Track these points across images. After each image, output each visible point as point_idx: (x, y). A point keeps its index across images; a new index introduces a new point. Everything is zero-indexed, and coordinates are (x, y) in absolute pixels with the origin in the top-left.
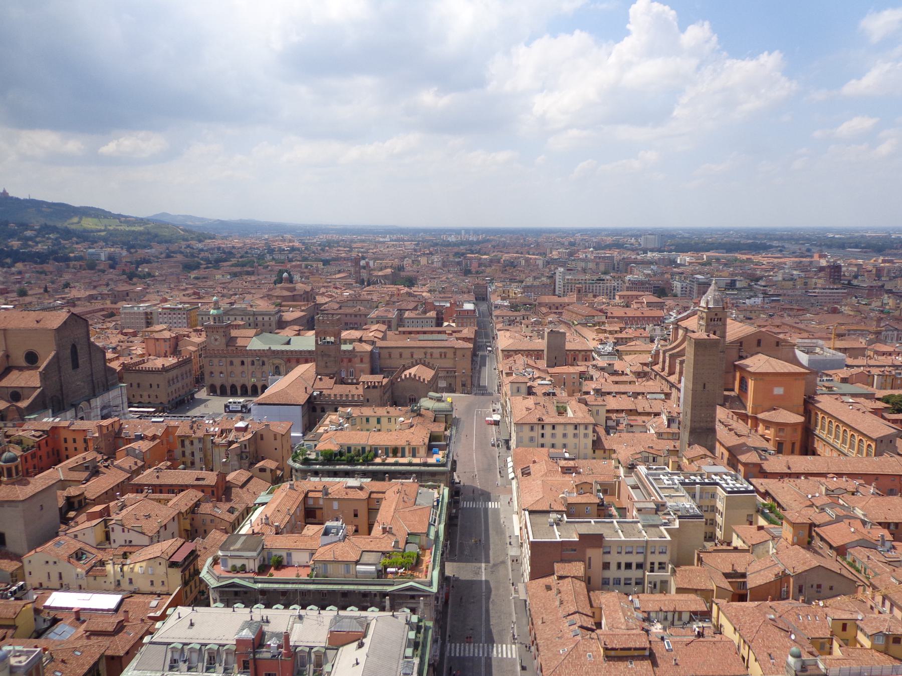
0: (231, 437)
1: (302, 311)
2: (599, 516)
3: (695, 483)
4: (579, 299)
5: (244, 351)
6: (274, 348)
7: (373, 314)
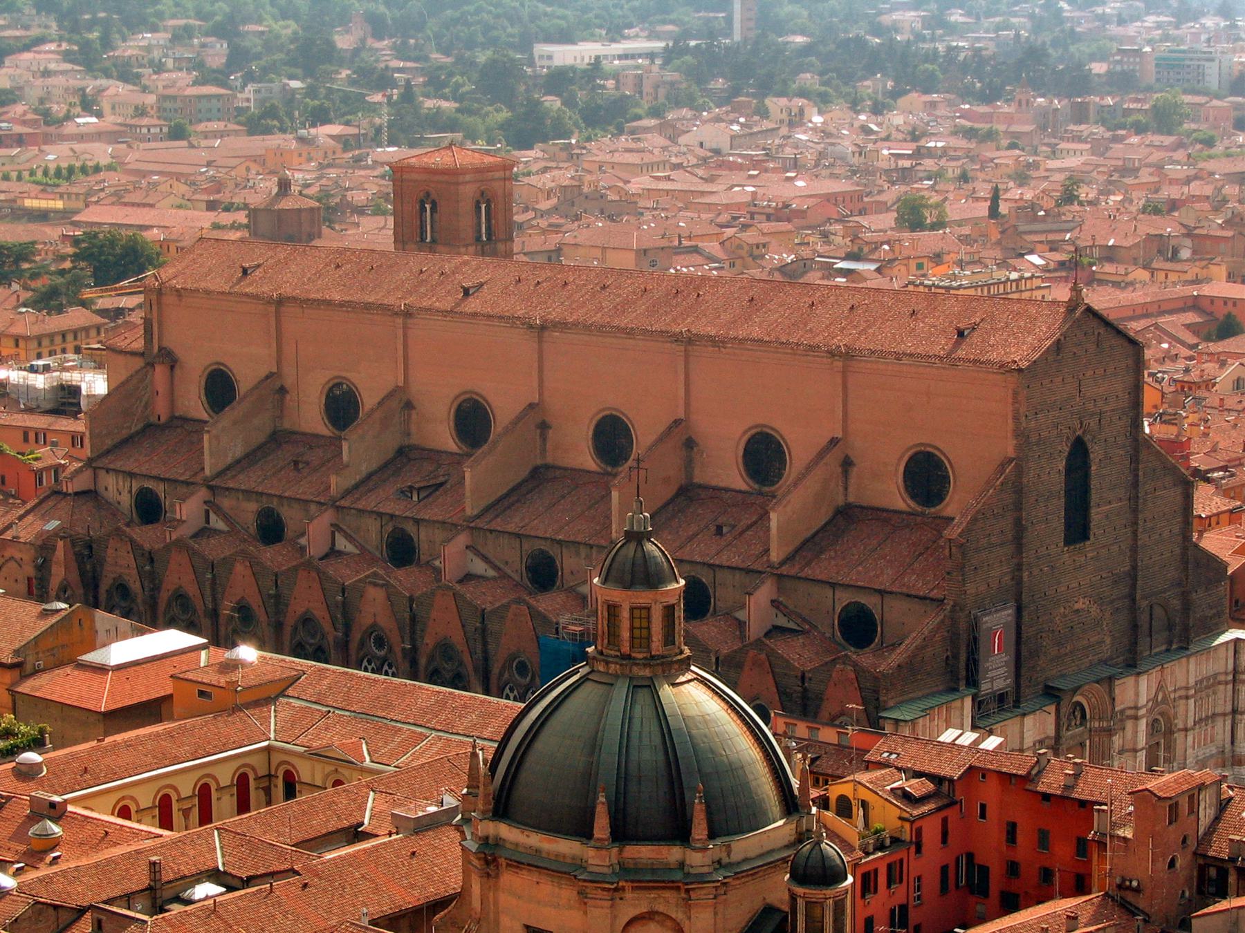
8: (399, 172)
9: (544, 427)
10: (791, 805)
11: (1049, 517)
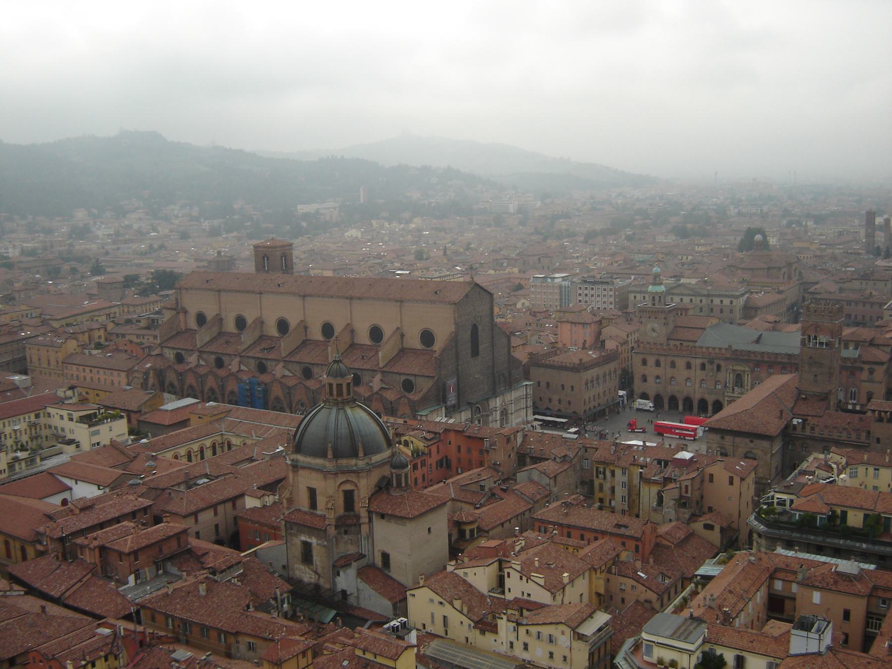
0: (669, 471)
6: (734, 347)
9: (306, 328)
10: (390, 444)
11: (466, 349)
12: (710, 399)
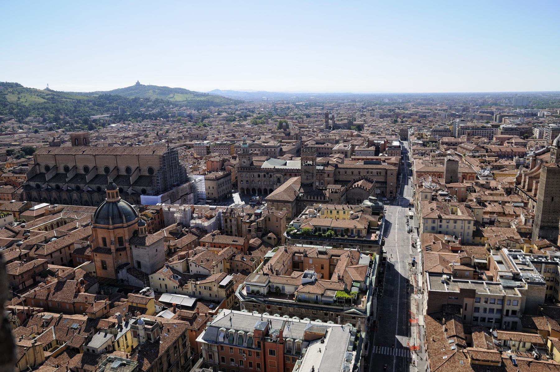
1: (294, 145)
2: (474, 279)
3: (541, 263)
4: (468, 140)
5: (259, 169)
7: (336, 147)
8: (71, 135)
12: (268, 188)
